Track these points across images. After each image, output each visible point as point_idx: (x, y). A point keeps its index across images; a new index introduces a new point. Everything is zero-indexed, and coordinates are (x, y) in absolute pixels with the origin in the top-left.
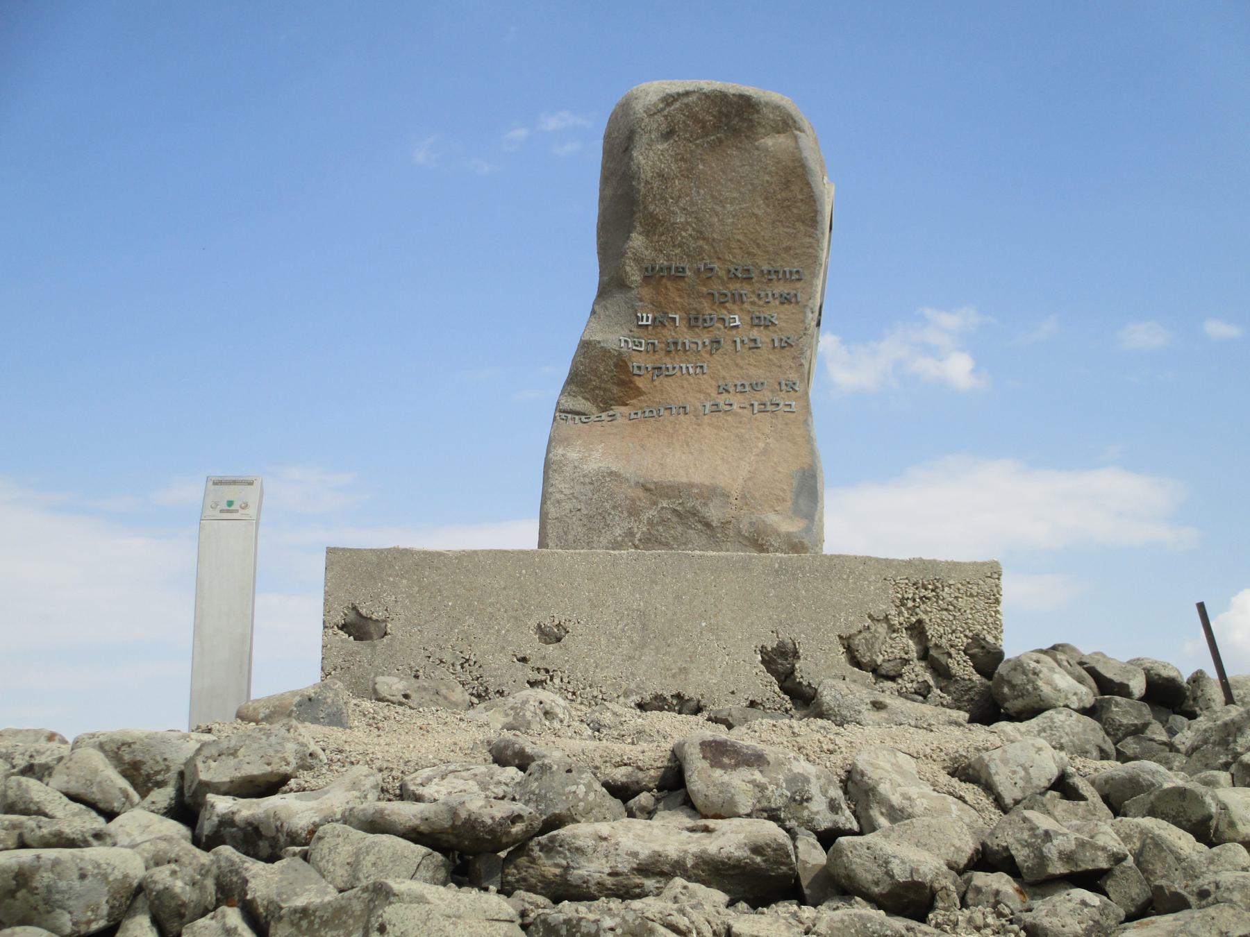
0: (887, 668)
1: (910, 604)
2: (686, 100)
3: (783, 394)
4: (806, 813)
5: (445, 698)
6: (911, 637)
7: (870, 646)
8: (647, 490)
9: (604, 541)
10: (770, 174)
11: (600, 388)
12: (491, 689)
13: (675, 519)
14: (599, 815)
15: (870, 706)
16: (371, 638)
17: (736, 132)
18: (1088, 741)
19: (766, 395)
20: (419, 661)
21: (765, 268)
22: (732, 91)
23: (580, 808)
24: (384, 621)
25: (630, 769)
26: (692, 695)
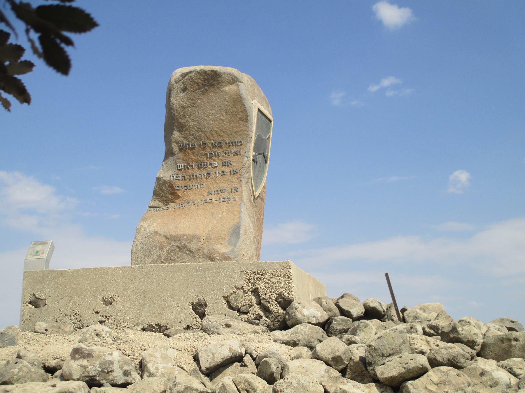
0: (243, 309)
1: (252, 281)
2: (190, 75)
3: (233, 194)
4: (110, 377)
5: (63, 330)
6: (254, 295)
7: (236, 300)
8: (167, 238)
9: (150, 260)
10: (227, 102)
11: (164, 196)
12: (84, 325)
13: (178, 250)
14: (23, 381)
15: (225, 326)
16: (40, 307)
17: (212, 86)
18: (313, 338)
19: (226, 195)
20: (58, 315)
21: (228, 141)
22: (208, 69)
23: (15, 378)
24: (45, 300)
25: (59, 360)
26: (164, 324)
